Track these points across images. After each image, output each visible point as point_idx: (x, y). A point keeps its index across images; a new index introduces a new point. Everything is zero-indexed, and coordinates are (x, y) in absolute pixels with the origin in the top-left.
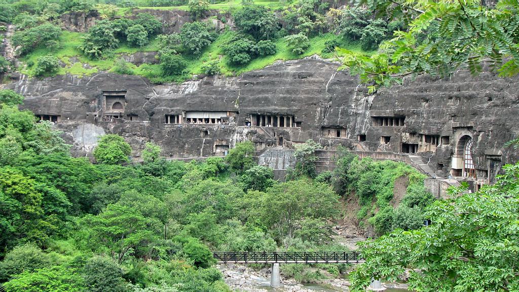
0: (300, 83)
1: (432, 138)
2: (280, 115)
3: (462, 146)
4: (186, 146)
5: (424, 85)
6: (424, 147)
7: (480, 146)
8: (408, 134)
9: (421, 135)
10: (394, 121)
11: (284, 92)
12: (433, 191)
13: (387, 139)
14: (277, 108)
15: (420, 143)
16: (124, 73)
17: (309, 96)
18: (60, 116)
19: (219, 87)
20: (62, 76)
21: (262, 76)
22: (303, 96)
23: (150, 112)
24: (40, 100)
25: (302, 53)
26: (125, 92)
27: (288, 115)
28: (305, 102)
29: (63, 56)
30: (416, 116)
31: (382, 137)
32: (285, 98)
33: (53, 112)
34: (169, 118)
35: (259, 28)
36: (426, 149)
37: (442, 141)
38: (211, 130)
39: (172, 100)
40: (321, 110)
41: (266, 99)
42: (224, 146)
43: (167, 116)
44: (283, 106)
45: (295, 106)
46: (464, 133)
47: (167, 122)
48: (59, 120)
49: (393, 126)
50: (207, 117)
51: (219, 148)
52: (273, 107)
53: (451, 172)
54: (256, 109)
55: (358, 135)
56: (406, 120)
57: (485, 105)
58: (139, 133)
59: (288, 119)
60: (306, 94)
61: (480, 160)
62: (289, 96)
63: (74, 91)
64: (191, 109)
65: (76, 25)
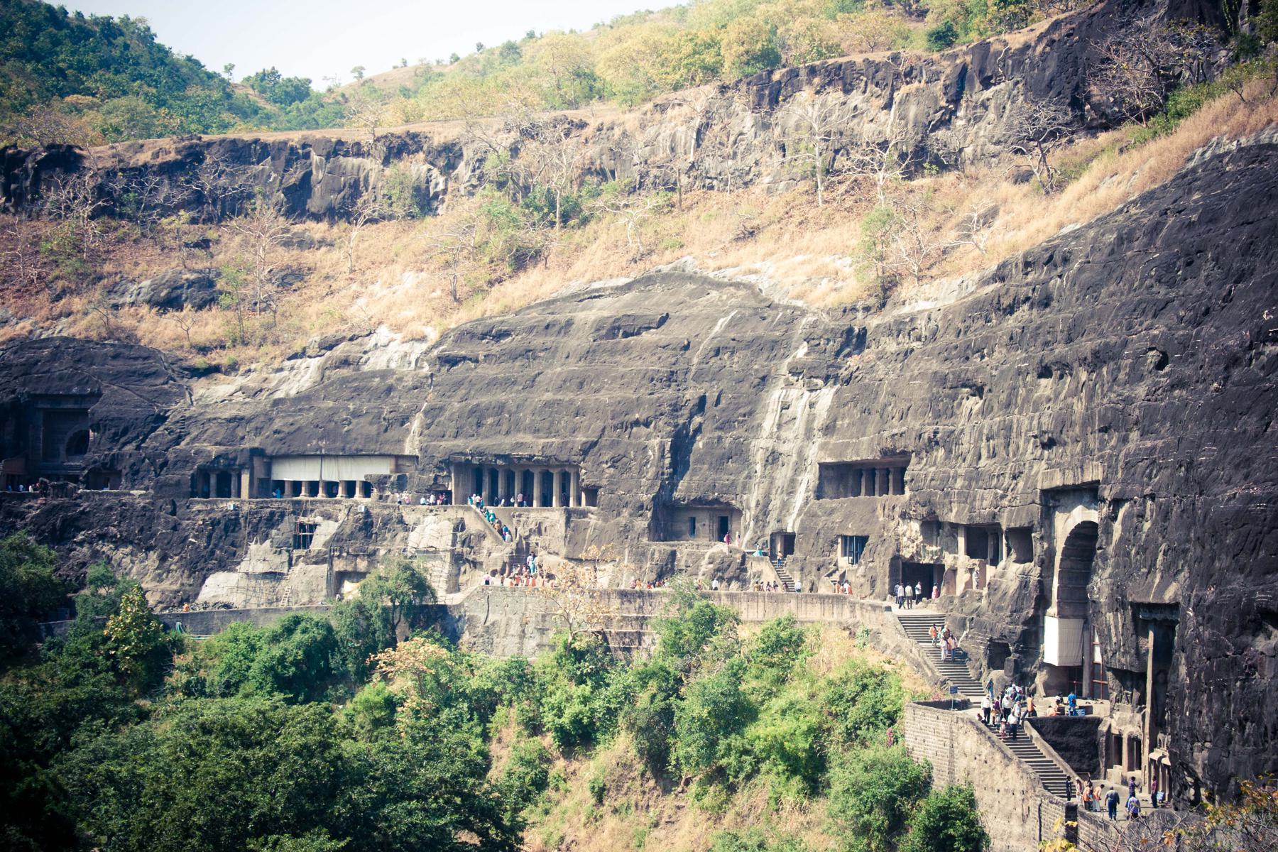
7: (1117, 566)
8: (916, 526)
9: (955, 527)
10: (891, 477)
15: (948, 560)
19: (374, 374)
23: (160, 461)
27: (562, 464)
34: (213, 481)
36: (968, 584)
37: (1009, 550)
39: (230, 420)
40: (662, 446)
43: (204, 473)
46: (1080, 514)
53: (1041, 678)
58: (113, 530)
59: (565, 478)
61: (1116, 627)
64: (283, 451)
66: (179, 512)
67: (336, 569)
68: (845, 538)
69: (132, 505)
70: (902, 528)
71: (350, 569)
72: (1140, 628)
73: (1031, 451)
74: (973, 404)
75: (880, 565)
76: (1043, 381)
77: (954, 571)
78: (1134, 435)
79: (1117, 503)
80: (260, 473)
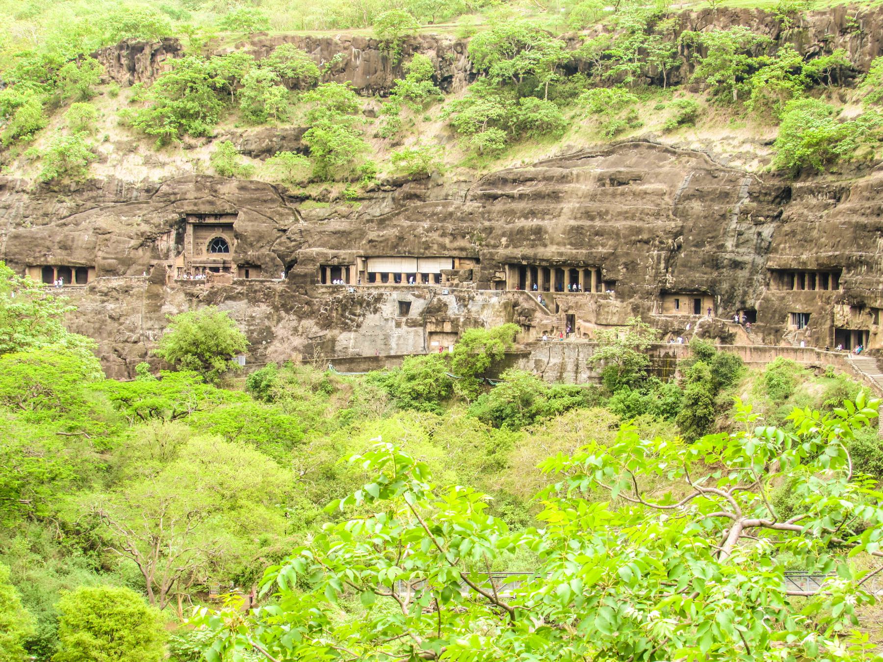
0: (614, 195)
2: (569, 265)
8: (847, 308)
10: (817, 278)
11: (579, 215)
14: (562, 249)
15: (872, 328)
17: (633, 223)
18: (93, 268)
21: (531, 180)
22: (621, 225)
23: (289, 259)
27: (586, 265)
28: (625, 238)
30: (864, 268)
31: (794, 314)
33: (79, 258)
40: (659, 257)
41: (538, 232)
42: (447, 333)
43: (323, 268)
45: (603, 245)
47: (324, 281)
48: (91, 277)
49: (817, 289)
50: (414, 271)
51: (435, 337)
54: (518, 252)
56: (845, 276)
59: (587, 274)
60: (626, 218)
62: (588, 223)
65: (132, 69)
66: (309, 292)
67: (428, 330)
68: (794, 314)
69: (275, 290)
70: (838, 308)
71: (438, 330)
77: (875, 334)
80: (360, 267)
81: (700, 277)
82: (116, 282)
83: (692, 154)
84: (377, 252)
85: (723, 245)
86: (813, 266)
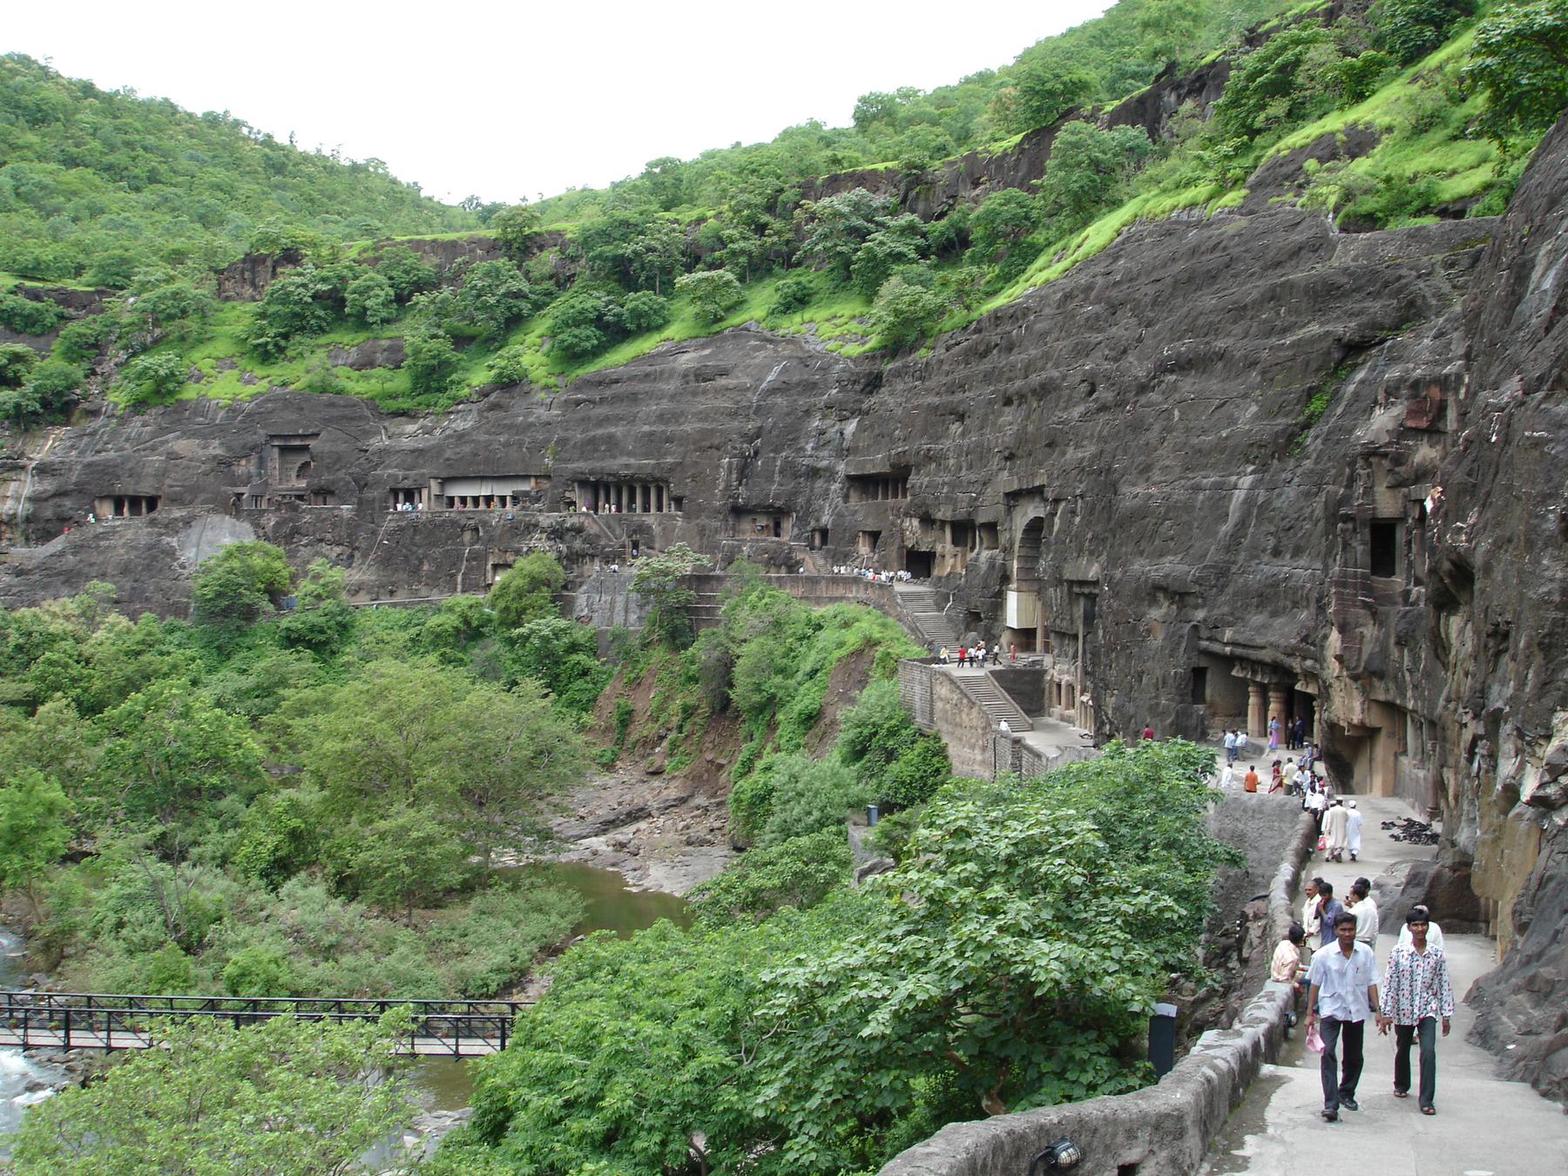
0: (695, 394)
1: (963, 531)
3: (1032, 553)
4: (426, 567)
5: (961, 372)
6: (950, 560)
7: (1056, 552)
8: (915, 522)
9: (943, 523)
12: (918, 705)
13: (874, 536)
14: (632, 461)
15: (939, 548)
16: (324, 391)
17: (706, 425)
20: (188, 401)
21: (616, 382)
24: (126, 459)
25: (721, 319)
26: (316, 435)
27: (656, 480)
29: (201, 358)
30: (933, 466)
32: (652, 434)
35: (631, 261)
36: (953, 567)
38: (485, 524)
39: (412, 452)
40: (730, 463)
41: (610, 440)
43: (395, 492)
44: (647, 456)
45: (672, 454)
52: (624, 460)
53: (1005, 638)
54: (582, 466)
55: (814, 530)
56: (913, 479)
57: (1077, 412)
58: (329, 536)
60: (701, 420)
63: (204, 437)
65: (254, 285)
72: (1073, 598)
73: (995, 462)
74: (956, 428)
75: (893, 552)
76: (1007, 409)
78: (1071, 450)
79: (1057, 501)
81: (774, 490)
82: (177, 513)
83: (791, 340)
84: (453, 473)
85: (803, 449)
86: (887, 469)
